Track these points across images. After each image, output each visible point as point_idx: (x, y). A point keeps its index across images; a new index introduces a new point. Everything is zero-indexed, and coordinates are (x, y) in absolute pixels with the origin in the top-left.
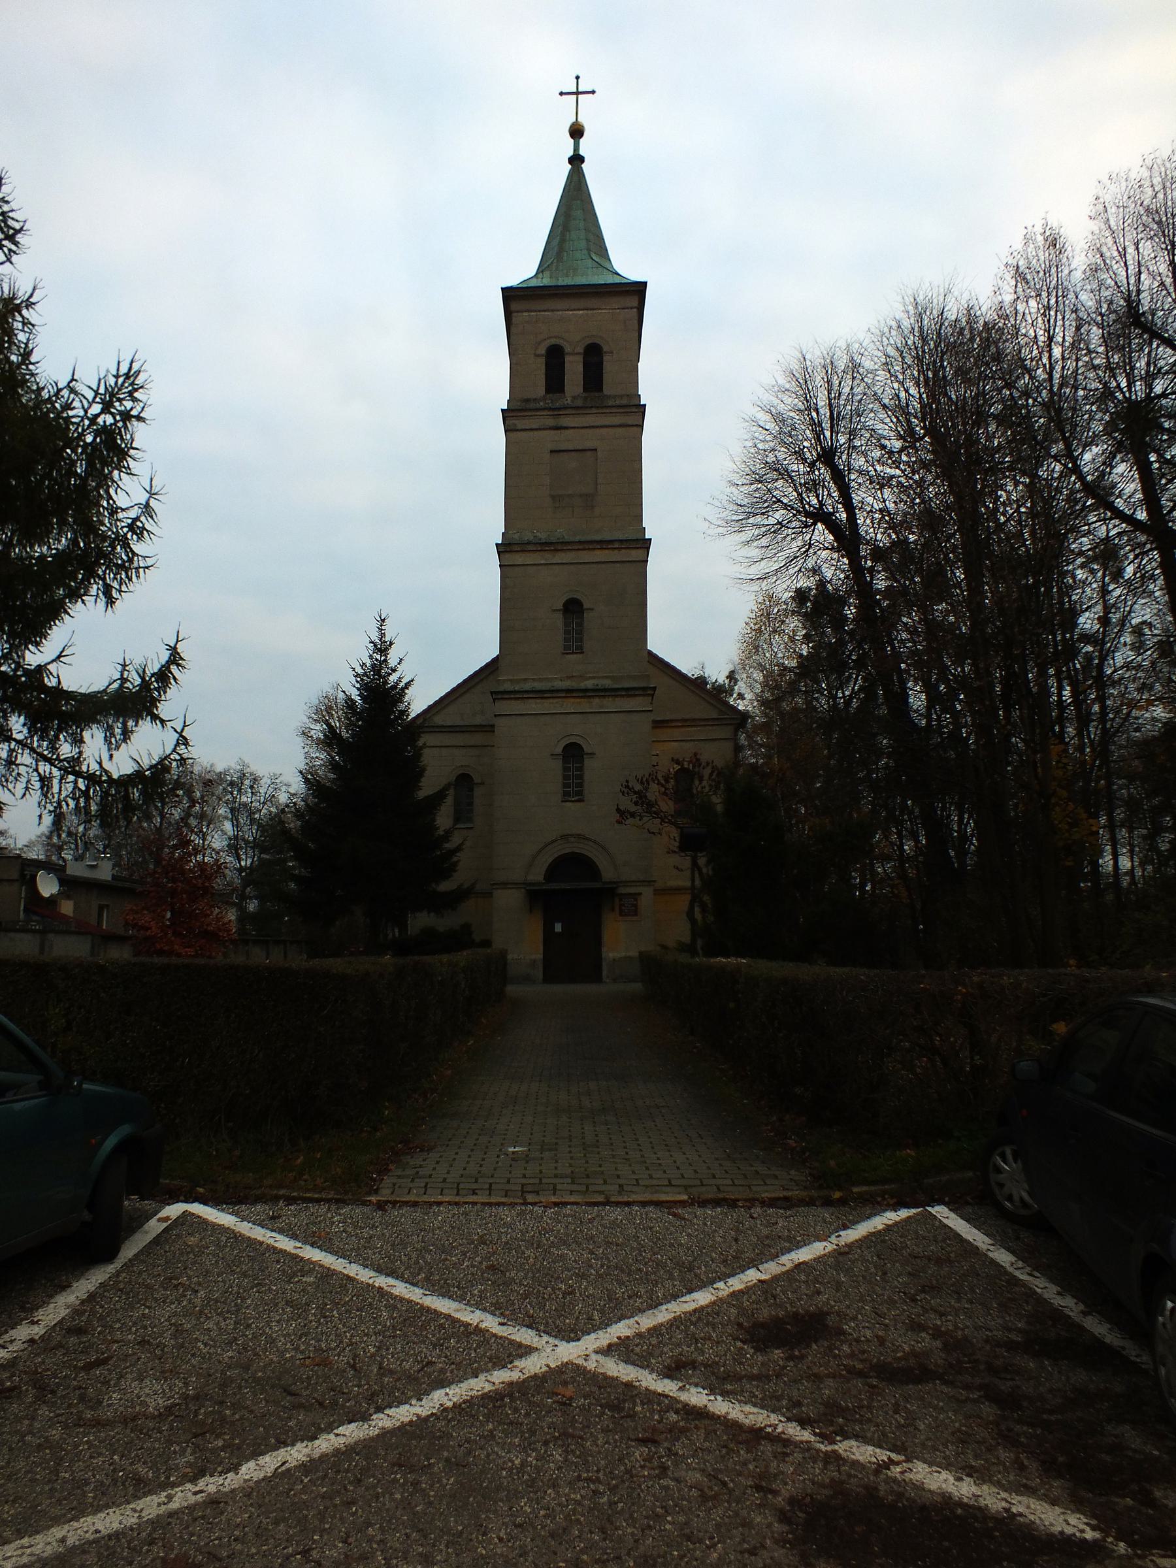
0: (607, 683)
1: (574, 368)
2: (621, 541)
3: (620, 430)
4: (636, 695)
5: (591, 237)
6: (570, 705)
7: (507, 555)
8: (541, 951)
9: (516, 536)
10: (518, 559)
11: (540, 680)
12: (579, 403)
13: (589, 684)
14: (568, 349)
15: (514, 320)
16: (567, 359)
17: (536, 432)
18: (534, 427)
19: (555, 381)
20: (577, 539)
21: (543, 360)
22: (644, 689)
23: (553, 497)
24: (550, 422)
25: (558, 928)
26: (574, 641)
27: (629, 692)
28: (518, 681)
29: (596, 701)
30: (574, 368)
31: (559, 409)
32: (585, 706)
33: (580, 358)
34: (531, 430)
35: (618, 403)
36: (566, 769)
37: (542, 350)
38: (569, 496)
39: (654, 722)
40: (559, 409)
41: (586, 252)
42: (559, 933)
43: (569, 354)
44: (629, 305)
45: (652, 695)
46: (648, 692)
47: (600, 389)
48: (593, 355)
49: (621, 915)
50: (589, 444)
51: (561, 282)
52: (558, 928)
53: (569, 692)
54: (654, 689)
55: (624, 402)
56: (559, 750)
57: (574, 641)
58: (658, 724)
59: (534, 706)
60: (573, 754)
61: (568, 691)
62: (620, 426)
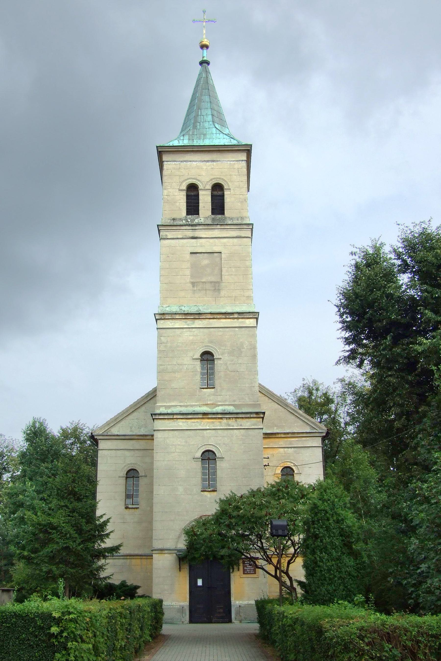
0: (231, 409)
1: (205, 200)
2: (239, 313)
3: (235, 240)
4: (251, 418)
5: (215, 113)
6: (206, 424)
7: (162, 321)
8: (188, 600)
9: (168, 309)
10: (169, 324)
11: (186, 406)
12: (209, 222)
13: (219, 409)
14: (201, 187)
15: (165, 167)
16: (201, 193)
17: (180, 240)
18: (179, 237)
19: (193, 207)
20: (209, 311)
21: (184, 193)
22: (257, 413)
23: (193, 284)
24: (190, 234)
25: (200, 582)
26: (209, 379)
27: (248, 415)
28: (170, 407)
29: (225, 421)
30: (205, 200)
31: (196, 225)
32: (217, 424)
33: (209, 193)
34: (178, 238)
35: (235, 222)
36: (203, 468)
37: (184, 187)
38: (203, 282)
39: (265, 434)
40: (196, 225)
41: (211, 123)
42: (200, 586)
43: (201, 190)
44: (242, 159)
45: (263, 418)
46: (260, 415)
47: (223, 213)
48: (218, 190)
49: (244, 573)
50: (216, 249)
51: (195, 143)
52: (200, 582)
53: (205, 415)
54: (264, 413)
55: (239, 222)
56: (199, 454)
57: (209, 379)
58: (267, 436)
59: (182, 424)
60: (209, 457)
61: (204, 414)
62: (236, 237)
